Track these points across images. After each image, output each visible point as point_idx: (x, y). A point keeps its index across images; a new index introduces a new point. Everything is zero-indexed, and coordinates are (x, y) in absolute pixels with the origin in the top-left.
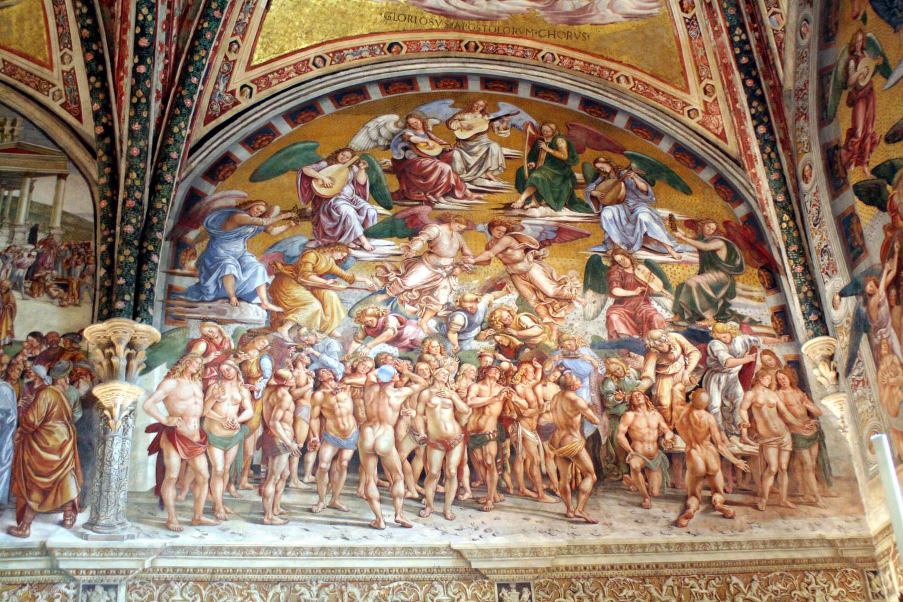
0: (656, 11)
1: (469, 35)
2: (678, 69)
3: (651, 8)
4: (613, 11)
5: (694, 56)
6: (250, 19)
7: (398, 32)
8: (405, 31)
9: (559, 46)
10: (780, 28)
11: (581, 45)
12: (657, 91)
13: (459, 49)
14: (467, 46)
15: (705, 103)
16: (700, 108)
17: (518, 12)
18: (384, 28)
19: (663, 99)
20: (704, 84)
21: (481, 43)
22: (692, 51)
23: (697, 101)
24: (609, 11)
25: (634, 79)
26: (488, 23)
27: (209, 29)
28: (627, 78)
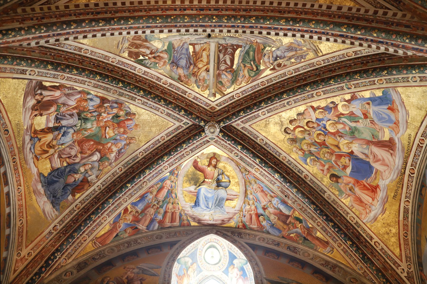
0: (49, 219)
1: (18, 157)
2: (33, 239)
3: (49, 216)
4: (43, 204)
5: (39, 242)
6: (8, 73)
7: (13, 131)
8: (14, 133)
9: (25, 192)
10: (62, 264)
11: (28, 199)
12: (22, 237)
13: (12, 156)
14: (14, 158)
15: (25, 256)
16: (22, 256)
17: (31, 170)
18: (13, 125)
19: (20, 241)
20: (31, 251)
21: (16, 163)
22: (41, 240)
23: (24, 253)
24: (43, 203)
25: (23, 226)
26: (24, 162)
27: (9, 61)
28: (22, 222)
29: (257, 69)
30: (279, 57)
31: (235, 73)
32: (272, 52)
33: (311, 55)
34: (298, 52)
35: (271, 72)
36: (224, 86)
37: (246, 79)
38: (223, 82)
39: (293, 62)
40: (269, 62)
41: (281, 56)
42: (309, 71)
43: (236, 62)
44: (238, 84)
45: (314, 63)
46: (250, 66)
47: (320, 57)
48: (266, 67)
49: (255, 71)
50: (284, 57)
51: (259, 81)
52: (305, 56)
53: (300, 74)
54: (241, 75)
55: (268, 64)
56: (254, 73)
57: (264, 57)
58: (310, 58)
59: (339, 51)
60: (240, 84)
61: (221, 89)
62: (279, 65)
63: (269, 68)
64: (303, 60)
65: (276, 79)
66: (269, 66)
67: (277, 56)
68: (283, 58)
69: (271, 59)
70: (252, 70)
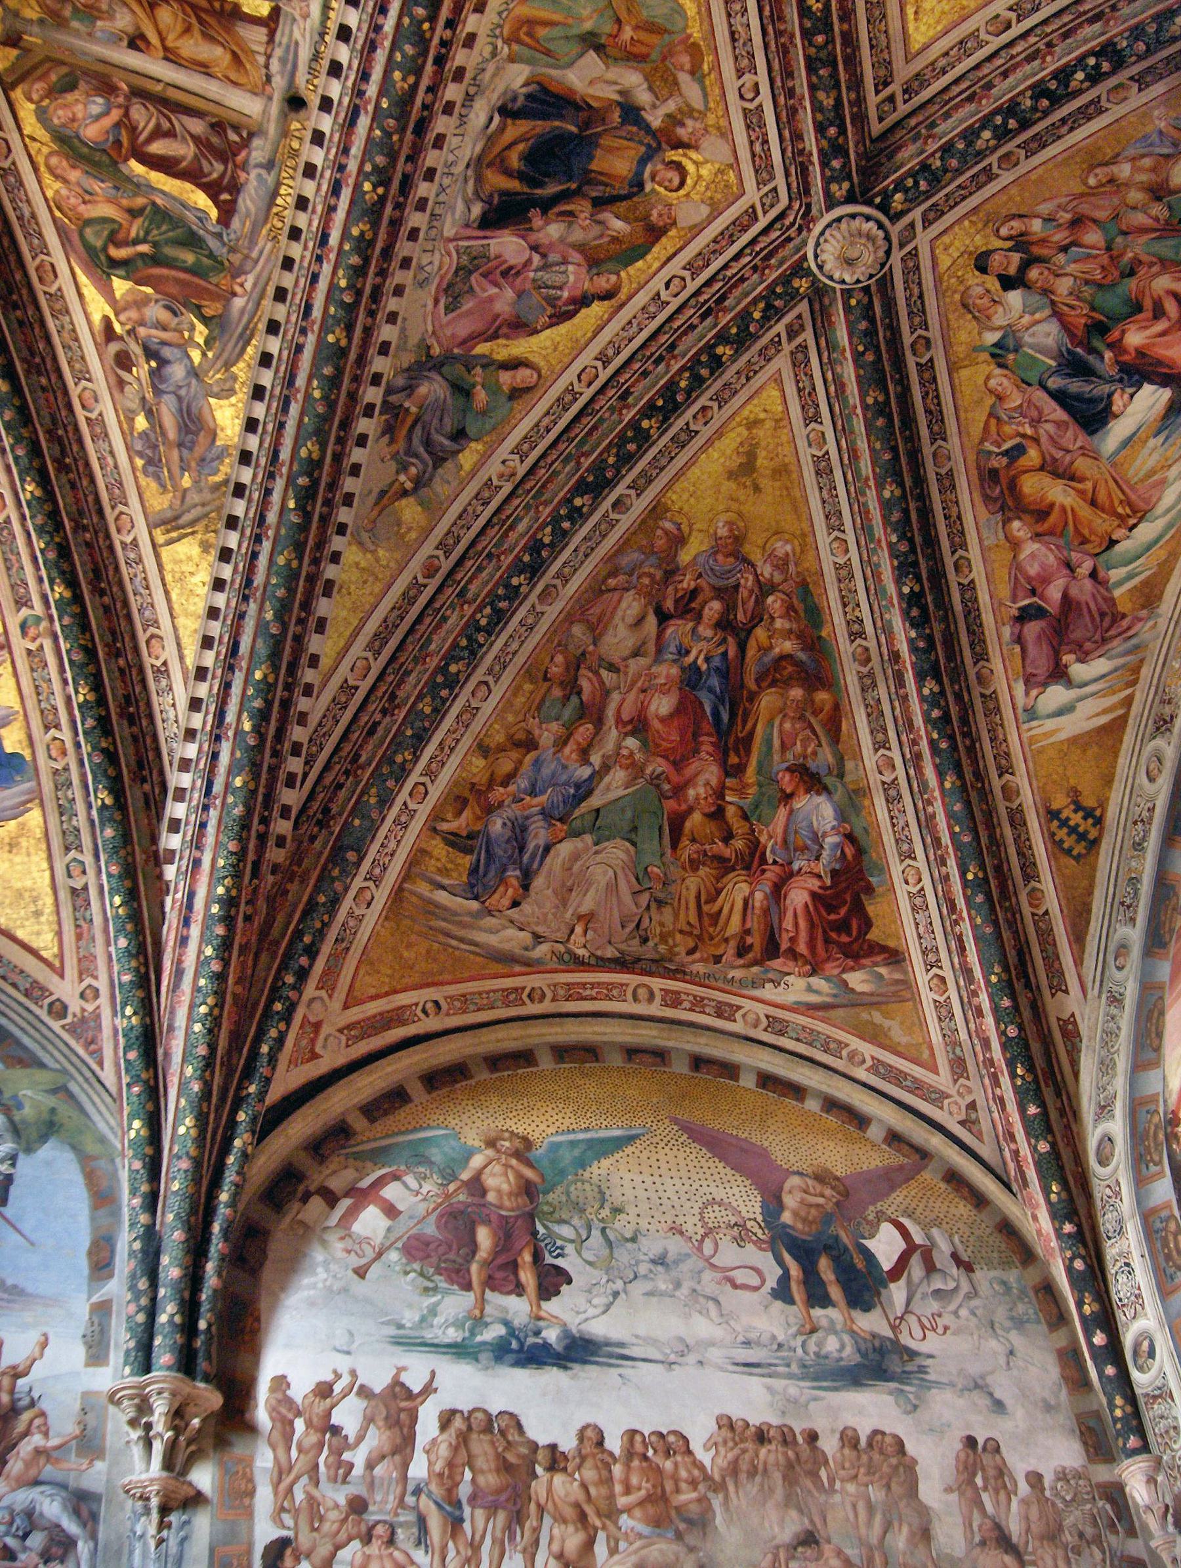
29: (114, 263)
30: (159, 368)
31: (105, 158)
32: (183, 346)
33: (160, 502)
34: (175, 454)
35: (97, 318)
36: (54, 92)
37: (73, 201)
38: (70, 97)
39: (133, 420)
40: (142, 323)
41: (163, 379)
42: (92, 481)
43: (158, 179)
44: (54, 161)
45: (126, 504)
46: (133, 234)
47: (150, 534)
48: (122, 304)
49: (105, 249)
50: (158, 392)
51: (58, 256)
52: (158, 478)
53: (80, 441)
54: (97, 186)
55: (133, 314)
56: (99, 244)
57: (167, 307)
58: (147, 495)
59: (171, 609)
60: (51, 171)
61: (39, 79)
62: (124, 361)
63: (117, 315)
64: (139, 462)
65: (65, 335)
66: (123, 318)
67: (163, 362)
68: (154, 386)
69: (154, 332)
70: (114, 239)
